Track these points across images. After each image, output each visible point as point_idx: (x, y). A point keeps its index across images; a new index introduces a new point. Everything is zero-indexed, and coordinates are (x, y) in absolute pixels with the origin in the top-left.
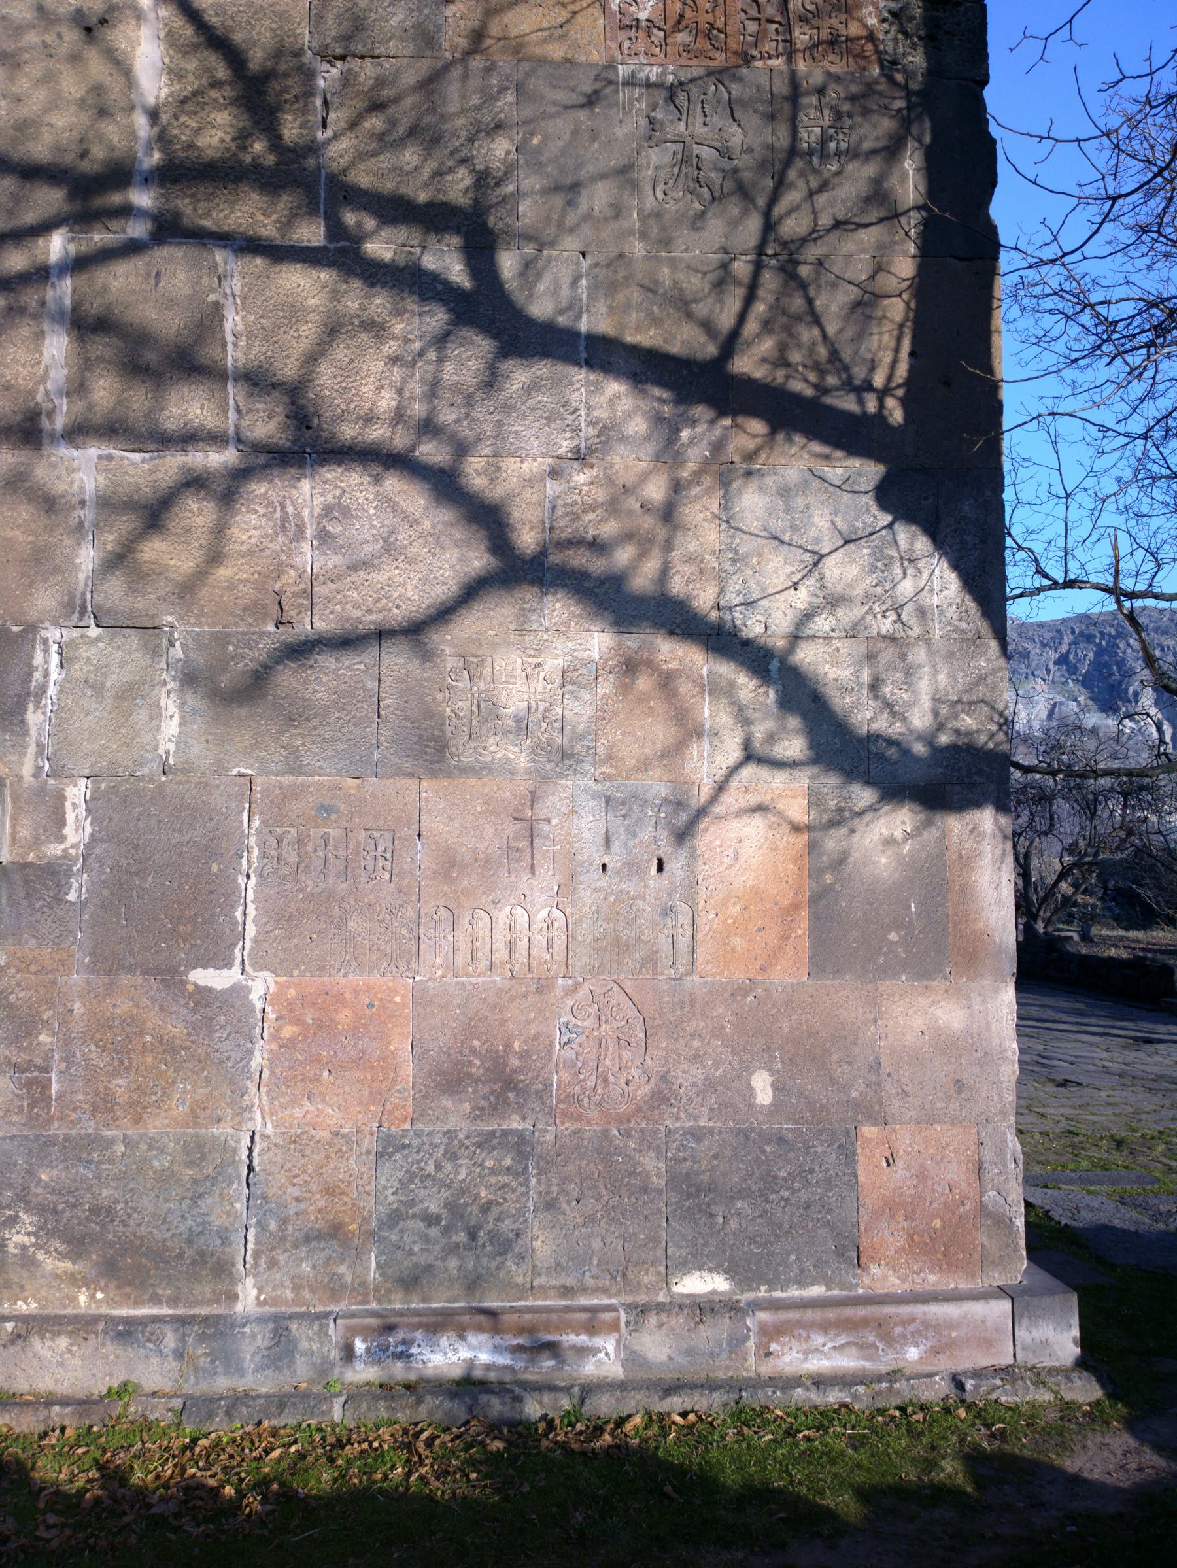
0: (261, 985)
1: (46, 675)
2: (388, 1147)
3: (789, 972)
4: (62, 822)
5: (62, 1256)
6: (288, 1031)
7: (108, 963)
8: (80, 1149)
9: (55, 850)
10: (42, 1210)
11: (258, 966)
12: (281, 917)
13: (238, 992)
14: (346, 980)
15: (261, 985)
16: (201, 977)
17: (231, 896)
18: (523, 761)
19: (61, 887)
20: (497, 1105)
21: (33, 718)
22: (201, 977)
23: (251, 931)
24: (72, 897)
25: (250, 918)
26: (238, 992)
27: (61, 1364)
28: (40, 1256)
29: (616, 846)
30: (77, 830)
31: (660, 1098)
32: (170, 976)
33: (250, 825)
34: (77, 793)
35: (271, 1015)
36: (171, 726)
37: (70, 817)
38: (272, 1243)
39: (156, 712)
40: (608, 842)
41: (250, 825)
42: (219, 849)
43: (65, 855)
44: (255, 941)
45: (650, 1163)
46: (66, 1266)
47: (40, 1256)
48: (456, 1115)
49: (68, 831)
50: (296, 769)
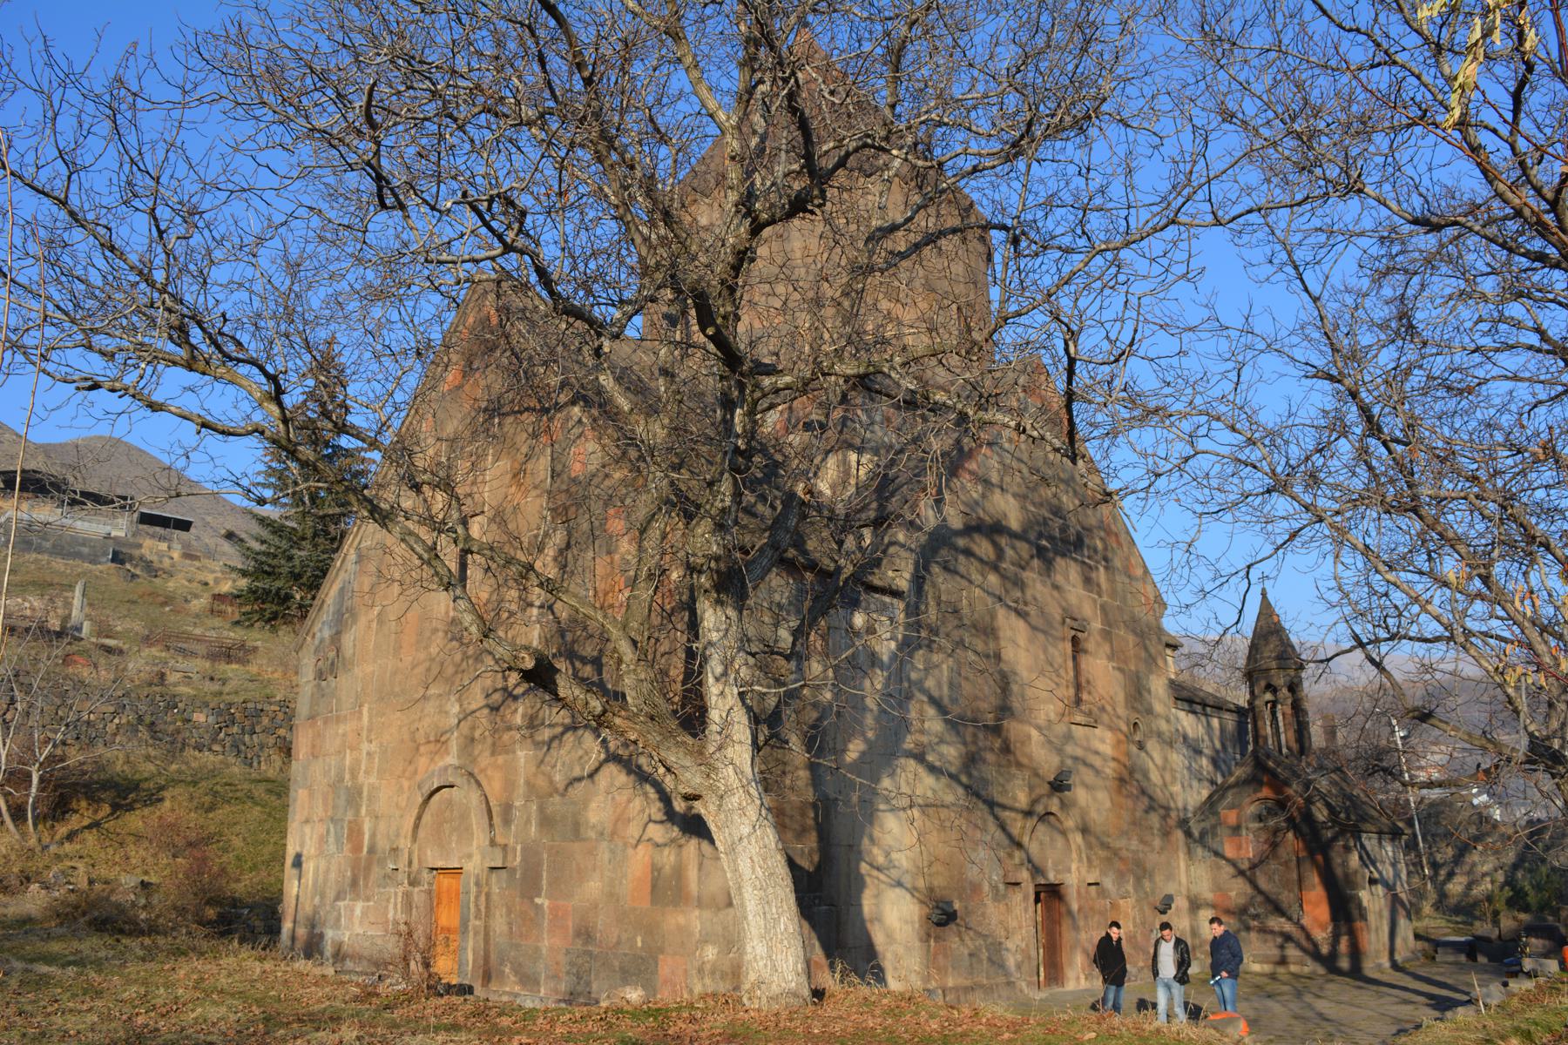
0: (546, 903)
2: (568, 952)
3: (645, 904)
7: (523, 896)
8: (517, 946)
12: (550, 884)
14: (561, 902)
16: (538, 901)
20: (586, 943)
30: (518, 859)
31: (618, 943)
38: (547, 977)
42: (540, 864)
45: (616, 963)
48: (579, 943)
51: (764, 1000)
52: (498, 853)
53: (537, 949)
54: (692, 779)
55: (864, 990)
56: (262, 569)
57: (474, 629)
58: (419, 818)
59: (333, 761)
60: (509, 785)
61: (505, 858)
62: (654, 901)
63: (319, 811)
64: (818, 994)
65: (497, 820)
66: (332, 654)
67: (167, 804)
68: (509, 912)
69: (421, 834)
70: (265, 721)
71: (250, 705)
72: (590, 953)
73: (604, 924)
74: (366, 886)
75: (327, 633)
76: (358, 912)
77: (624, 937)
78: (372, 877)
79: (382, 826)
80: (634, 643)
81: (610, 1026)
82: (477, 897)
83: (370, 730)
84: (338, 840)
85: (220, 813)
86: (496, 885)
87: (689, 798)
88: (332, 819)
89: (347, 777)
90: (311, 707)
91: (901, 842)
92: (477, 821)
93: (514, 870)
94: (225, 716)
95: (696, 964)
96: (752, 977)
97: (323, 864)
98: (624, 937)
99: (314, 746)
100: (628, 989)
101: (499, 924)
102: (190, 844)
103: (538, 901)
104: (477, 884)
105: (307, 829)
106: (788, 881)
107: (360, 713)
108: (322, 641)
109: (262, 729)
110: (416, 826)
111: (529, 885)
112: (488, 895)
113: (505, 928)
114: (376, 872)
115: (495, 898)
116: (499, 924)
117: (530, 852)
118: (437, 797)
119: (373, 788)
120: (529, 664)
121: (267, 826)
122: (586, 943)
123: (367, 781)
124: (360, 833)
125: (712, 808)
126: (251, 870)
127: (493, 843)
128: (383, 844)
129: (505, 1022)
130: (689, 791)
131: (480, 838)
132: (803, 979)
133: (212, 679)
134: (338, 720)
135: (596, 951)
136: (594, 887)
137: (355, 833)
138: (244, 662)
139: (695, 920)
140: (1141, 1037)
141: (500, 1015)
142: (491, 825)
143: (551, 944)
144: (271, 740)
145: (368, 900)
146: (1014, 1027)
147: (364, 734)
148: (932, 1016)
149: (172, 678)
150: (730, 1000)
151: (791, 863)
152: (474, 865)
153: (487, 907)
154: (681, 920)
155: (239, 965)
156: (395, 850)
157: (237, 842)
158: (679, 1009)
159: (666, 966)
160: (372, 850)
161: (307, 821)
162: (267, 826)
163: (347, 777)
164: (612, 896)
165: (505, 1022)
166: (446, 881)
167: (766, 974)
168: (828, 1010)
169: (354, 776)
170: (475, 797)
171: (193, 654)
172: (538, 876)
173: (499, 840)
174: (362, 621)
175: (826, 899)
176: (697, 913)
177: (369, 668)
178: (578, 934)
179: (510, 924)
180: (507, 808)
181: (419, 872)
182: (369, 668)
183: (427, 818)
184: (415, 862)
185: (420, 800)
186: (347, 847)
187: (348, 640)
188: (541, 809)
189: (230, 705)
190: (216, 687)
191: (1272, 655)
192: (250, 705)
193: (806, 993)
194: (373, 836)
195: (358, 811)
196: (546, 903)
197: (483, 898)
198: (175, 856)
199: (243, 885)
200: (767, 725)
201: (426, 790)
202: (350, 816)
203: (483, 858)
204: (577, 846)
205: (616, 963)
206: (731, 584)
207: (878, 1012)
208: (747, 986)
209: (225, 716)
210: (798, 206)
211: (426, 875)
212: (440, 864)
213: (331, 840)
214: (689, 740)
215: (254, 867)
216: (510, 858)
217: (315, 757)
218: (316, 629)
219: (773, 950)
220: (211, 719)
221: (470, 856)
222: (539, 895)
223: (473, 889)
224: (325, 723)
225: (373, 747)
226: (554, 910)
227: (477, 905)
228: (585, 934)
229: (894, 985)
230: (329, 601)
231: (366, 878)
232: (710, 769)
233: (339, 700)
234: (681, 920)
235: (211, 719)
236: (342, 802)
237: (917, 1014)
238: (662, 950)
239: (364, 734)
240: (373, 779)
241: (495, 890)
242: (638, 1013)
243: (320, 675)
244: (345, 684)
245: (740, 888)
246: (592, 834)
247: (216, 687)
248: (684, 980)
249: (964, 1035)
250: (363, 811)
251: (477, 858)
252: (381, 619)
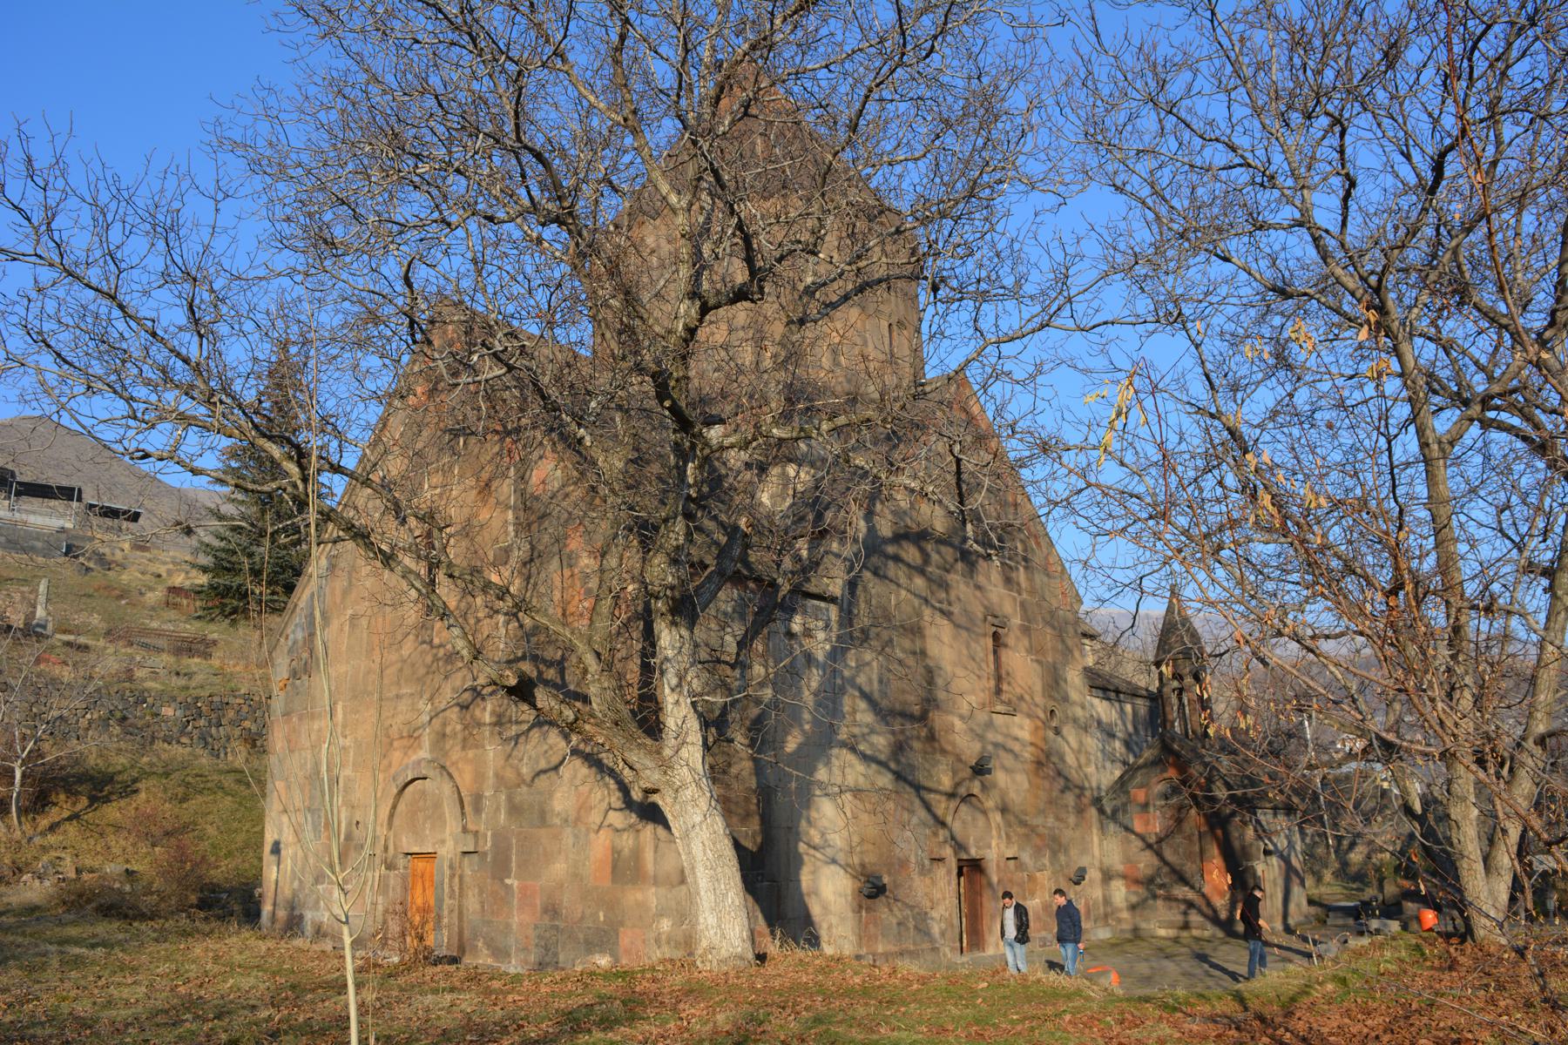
0: (516, 883)
2: (536, 927)
3: (607, 883)
7: (494, 877)
8: (489, 923)
12: (519, 866)
16: (508, 881)
20: (552, 919)
31: (582, 918)
32: (502, 880)
38: (517, 950)
42: (509, 848)
45: (581, 936)
48: (546, 921)
51: (715, 963)
52: (470, 838)
53: (508, 926)
54: (652, 777)
55: (800, 953)
56: (223, 565)
57: (465, 652)
58: (394, 807)
60: (479, 777)
61: (476, 843)
62: (614, 881)
64: (761, 958)
65: (468, 809)
66: (305, 655)
67: (143, 795)
68: (481, 892)
69: (397, 821)
70: (231, 714)
71: (216, 699)
72: (556, 928)
73: (569, 902)
75: (300, 635)
77: (588, 912)
80: (598, 655)
81: (586, 985)
82: (452, 876)
83: (344, 726)
85: (194, 804)
86: (469, 868)
87: (648, 792)
91: (836, 825)
92: (450, 810)
93: (485, 854)
94: (193, 710)
95: (653, 935)
96: (704, 944)
98: (588, 912)
100: (597, 956)
101: (472, 903)
102: (167, 834)
103: (508, 881)
104: (451, 867)
106: (735, 862)
108: (295, 642)
109: (236, 727)
110: (391, 816)
111: (500, 867)
112: (461, 877)
113: (478, 907)
115: (467, 879)
116: (472, 903)
117: (500, 839)
118: (411, 787)
119: (348, 779)
120: (513, 682)
121: (239, 815)
122: (552, 919)
125: (669, 800)
126: (226, 856)
127: (465, 830)
129: (496, 984)
130: (648, 785)
131: (452, 825)
132: (748, 945)
133: (178, 674)
134: (313, 717)
135: (561, 925)
136: (559, 868)
138: (207, 655)
139: (652, 896)
140: (1024, 987)
141: (491, 979)
142: (463, 814)
143: (520, 921)
144: (237, 732)
146: (923, 980)
148: (856, 973)
149: (140, 674)
150: (687, 964)
151: (737, 845)
152: (448, 851)
153: (461, 888)
154: (639, 896)
155: (237, 943)
157: (211, 831)
158: (643, 971)
159: (626, 938)
162: (239, 815)
164: (576, 876)
165: (496, 984)
166: (421, 865)
167: (716, 941)
168: (769, 969)
170: (447, 788)
171: (159, 650)
172: (508, 860)
173: (470, 827)
175: (768, 876)
176: (653, 890)
177: (343, 668)
178: (545, 911)
179: (482, 903)
180: (478, 798)
181: (395, 856)
182: (343, 668)
183: (401, 807)
184: (391, 848)
185: (395, 791)
188: (510, 799)
189: (197, 699)
190: (182, 682)
191: (1176, 642)
192: (216, 699)
193: (750, 956)
196: (516, 883)
197: (457, 880)
198: (154, 845)
199: (222, 871)
200: (715, 724)
201: (401, 781)
203: (456, 843)
204: (543, 831)
205: (581, 936)
206: (685, 609)
207: (811, 970)
208: (700, 952)
209: (193, 710)
210: (740, 295)
211: (401, 862)
212: (416, 849)
214: (649, 741)
215: (229, 854)
216: (481, 842)
217: (291, 751)
218: (289, 631)
219: (722, 920)
220: (178, 713)
221: (443, 842)
223: (447, 872)
224: (300, 719)
225: (348, 742)
226: (523, 889)
227: (451, 886)
228: (552, 910)
229: (828, 950)
230: (302, 604)
232: (666, 766)
234: (639, 896)
235: (178, 713)
237: (844, 971)
238: (622, 923)
241: (468, 872)
242: (608, 975)
243: (294, 674)
244: (321, 684)
245: (693, 868)
246: (557, 821)
247: (182, 682)
248: (645, 947)
249: (881, 986)
251: (450, 844)
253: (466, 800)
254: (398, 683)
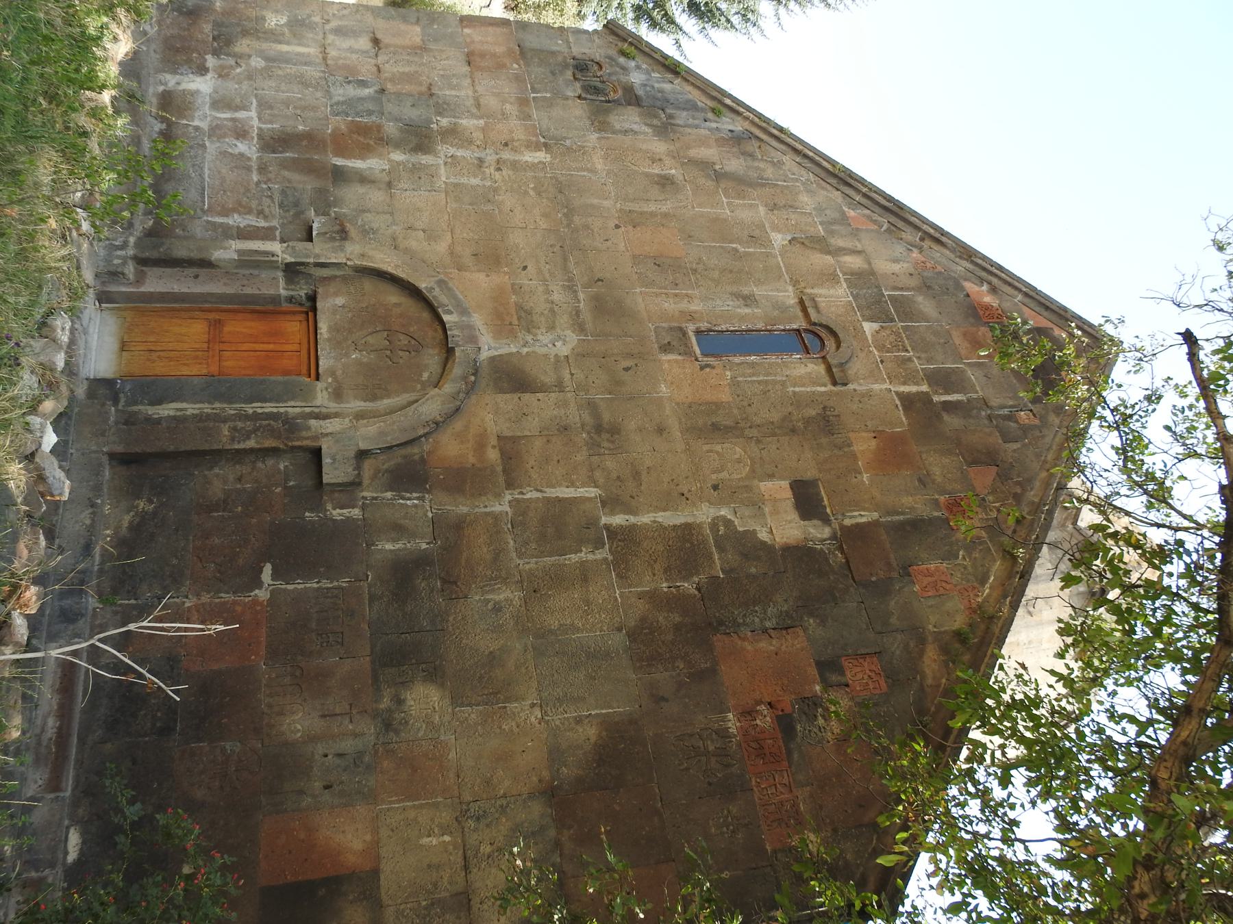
0: (262, 594)
1: (409, 499)
4: (341, 508)
5: (131, 523)
6: (239, 609)
9: (329, 507)
10: (155, 513)
11: (272, 592)
13: (259, 584)
15: (262, 594)
16: (267, 570)
17: (307, 577)
18: (382, 706)
19: (311, 510)
21: (389, 495)
22: (267, 570)
23: (290, 587)
24: (307, 514)
25: (299, 586)
26: (259, 584)
27: (77, 522)
28: (132, 514)
29: (338, 761)
30: (337, 514)
33: (344, 582)
34: (356, 513)
35: (247, 600)
36: (389, 546)
37: (345, 511)
39: (394, 541)
40: (340, 755)
41: (344, 582)
43: (326, 510)
44: (285, 590)
46: (125, 524)
47: (132, 514)
49: (338, 511)
50: (372, 599)
59: (466, 92)
63: (390, 69)
69: (368, 284)
74: (284, 165)
76: (242, 147)
78: (295, 177)
79: (376, 196)
83: (514, 165)
84: (350, 103)
88: (383, 91)
89: (444, 122)
90: (538, 52)
97: (313, 72)
99: (483, 55)
105: (364, 43)
107: (537, 147)
114: (306, 185)
123: (438, 159)
124: (365, 151)
127: (362, 455)
128: (351, 195)
131: (368, 435)
137: (365, 137)
145: (262, 169)
147: (507, 155)
156: (343, 234)
160: (339, 175)
161: (376, 42)
163: (444, 122)
169: (452, 134)
170: (432, 406)
173: (368, 466)
174: (660, 147)
184: (325, 272)
185: (422, 285)
186: (338, 123)
187: (629, 118)
194: (364, 179)
195: (398, 145)
202: (391, 128)
213: (352, 91)
222: (275, 576)
231: (295, 165)
233: (549, 104)
236: (412, 114)
239: (507, 155)
240: (444, 176)
246: (385, 703)
250: (398, 156)
252: (665, 182)
253: (415, 450)
254: (586, 286)
